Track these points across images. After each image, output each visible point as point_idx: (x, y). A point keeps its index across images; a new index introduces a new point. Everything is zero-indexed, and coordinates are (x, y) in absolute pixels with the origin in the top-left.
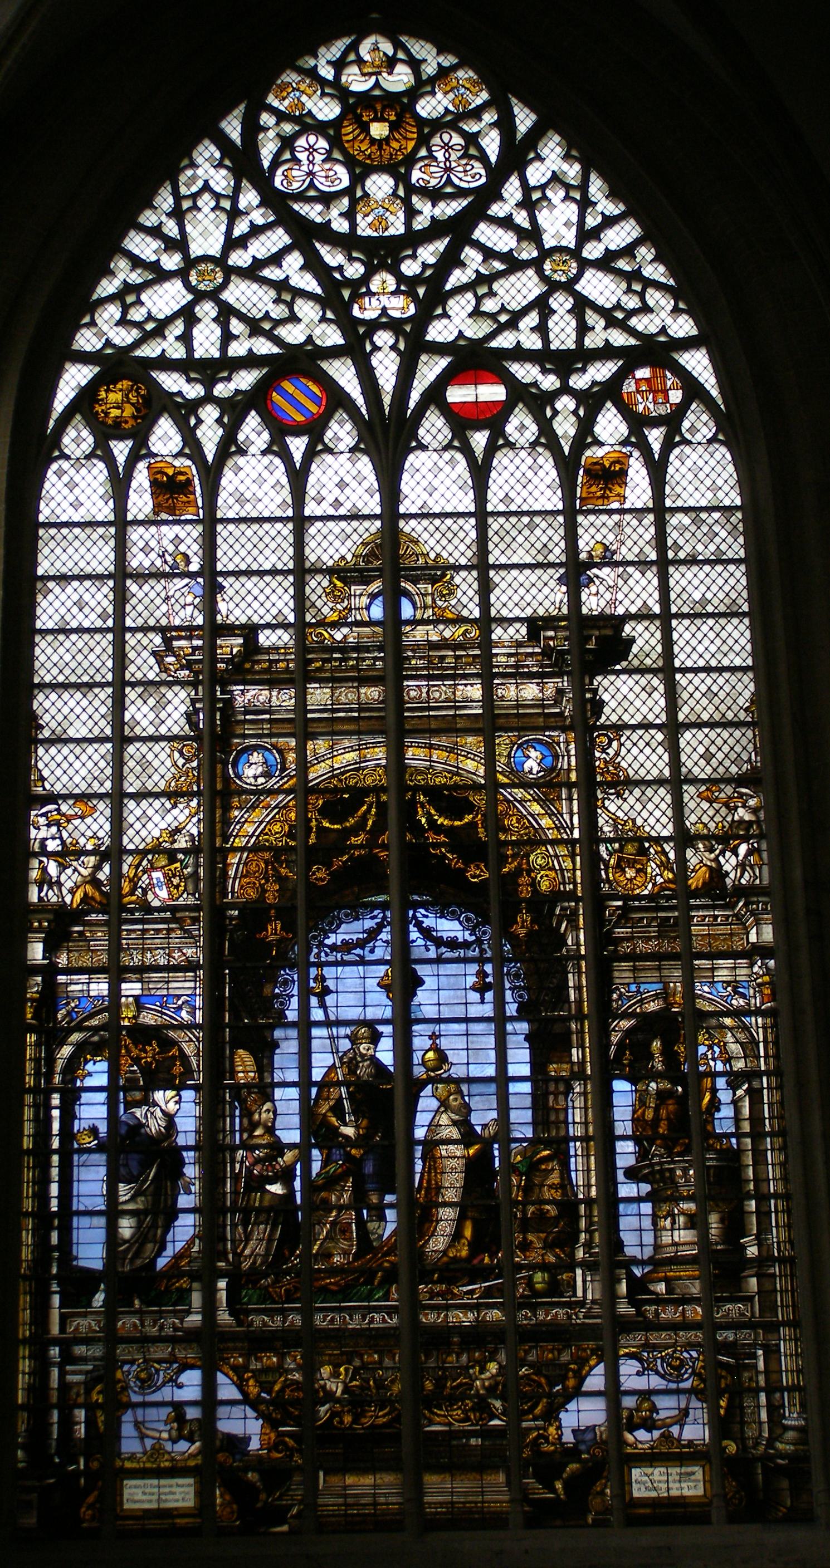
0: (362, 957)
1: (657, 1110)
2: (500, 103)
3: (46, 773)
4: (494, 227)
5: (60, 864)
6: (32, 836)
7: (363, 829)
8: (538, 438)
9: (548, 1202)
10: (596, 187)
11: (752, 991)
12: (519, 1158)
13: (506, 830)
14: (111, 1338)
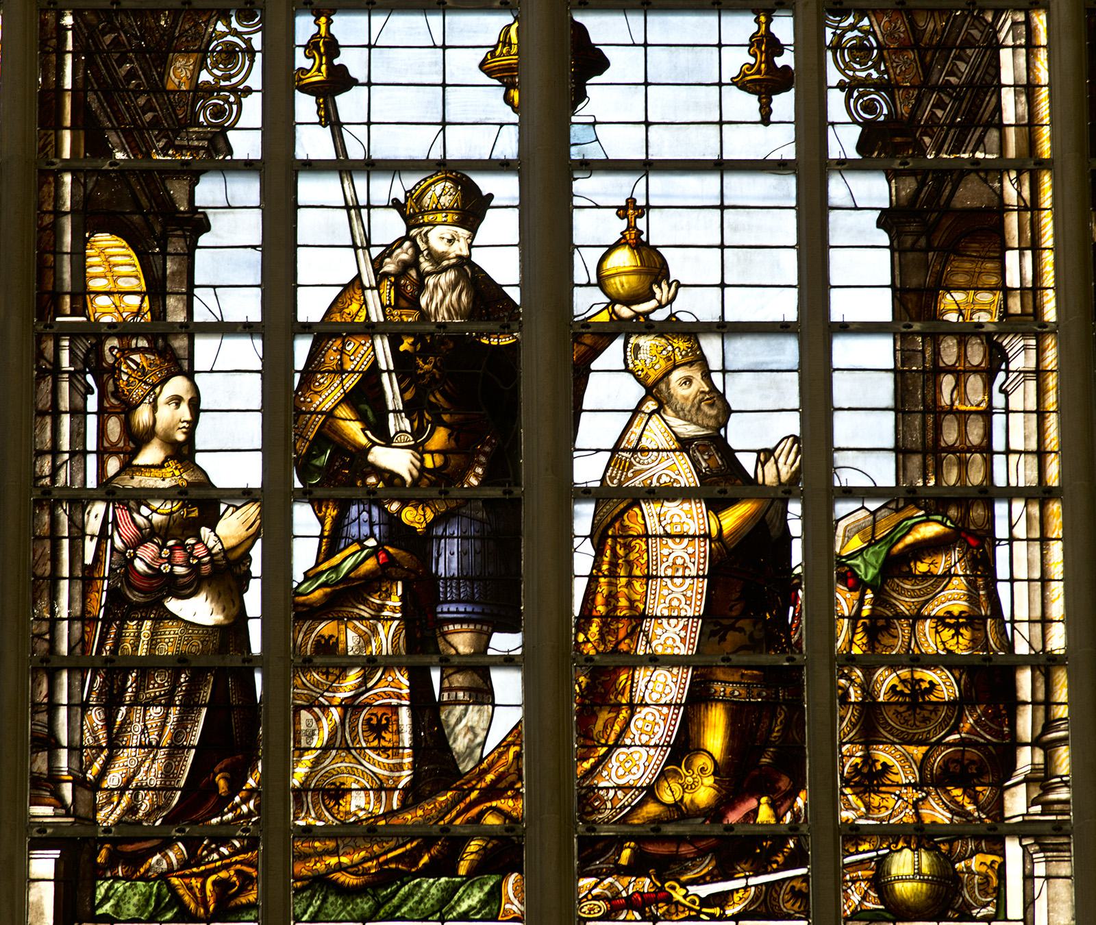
9: (931, 662)
12: (856, 543)
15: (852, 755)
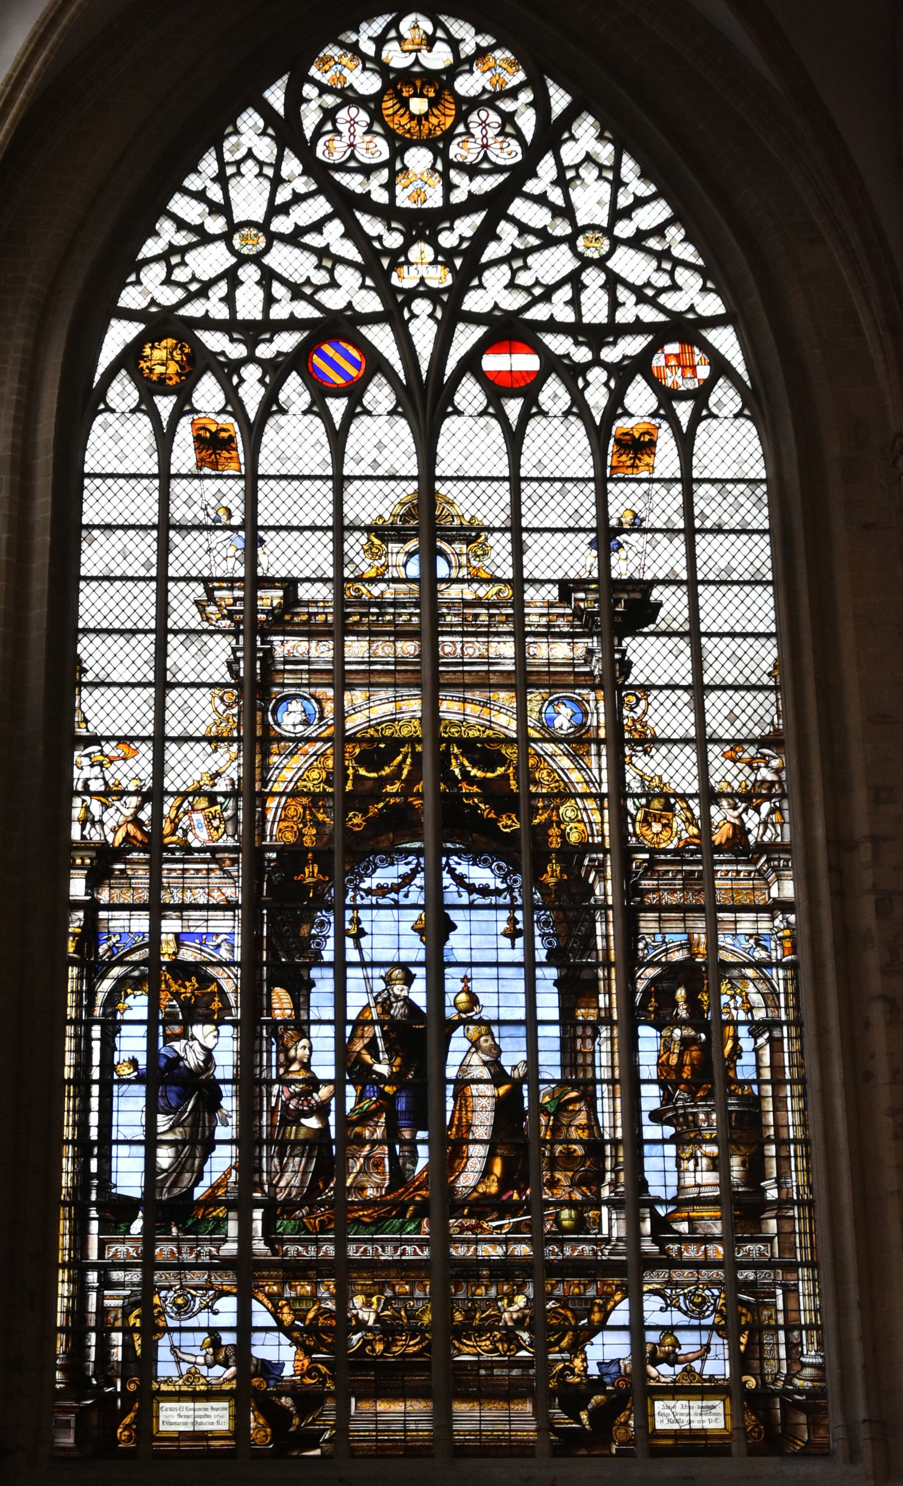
0: (396, 902)
1: (681, 1055)
2: (535, 83)
3: (89, 716)
4: (529, 204)
5: (103, 804)
6: (76, 776)
7: (399, 779)
8: (571, 407)
9: (575, 1142)
10: (629, 168)
11: (773, 944)
12: (547, 1099)
13: (537, 783)
14: (149, 1264)
15: (547, 1175)
